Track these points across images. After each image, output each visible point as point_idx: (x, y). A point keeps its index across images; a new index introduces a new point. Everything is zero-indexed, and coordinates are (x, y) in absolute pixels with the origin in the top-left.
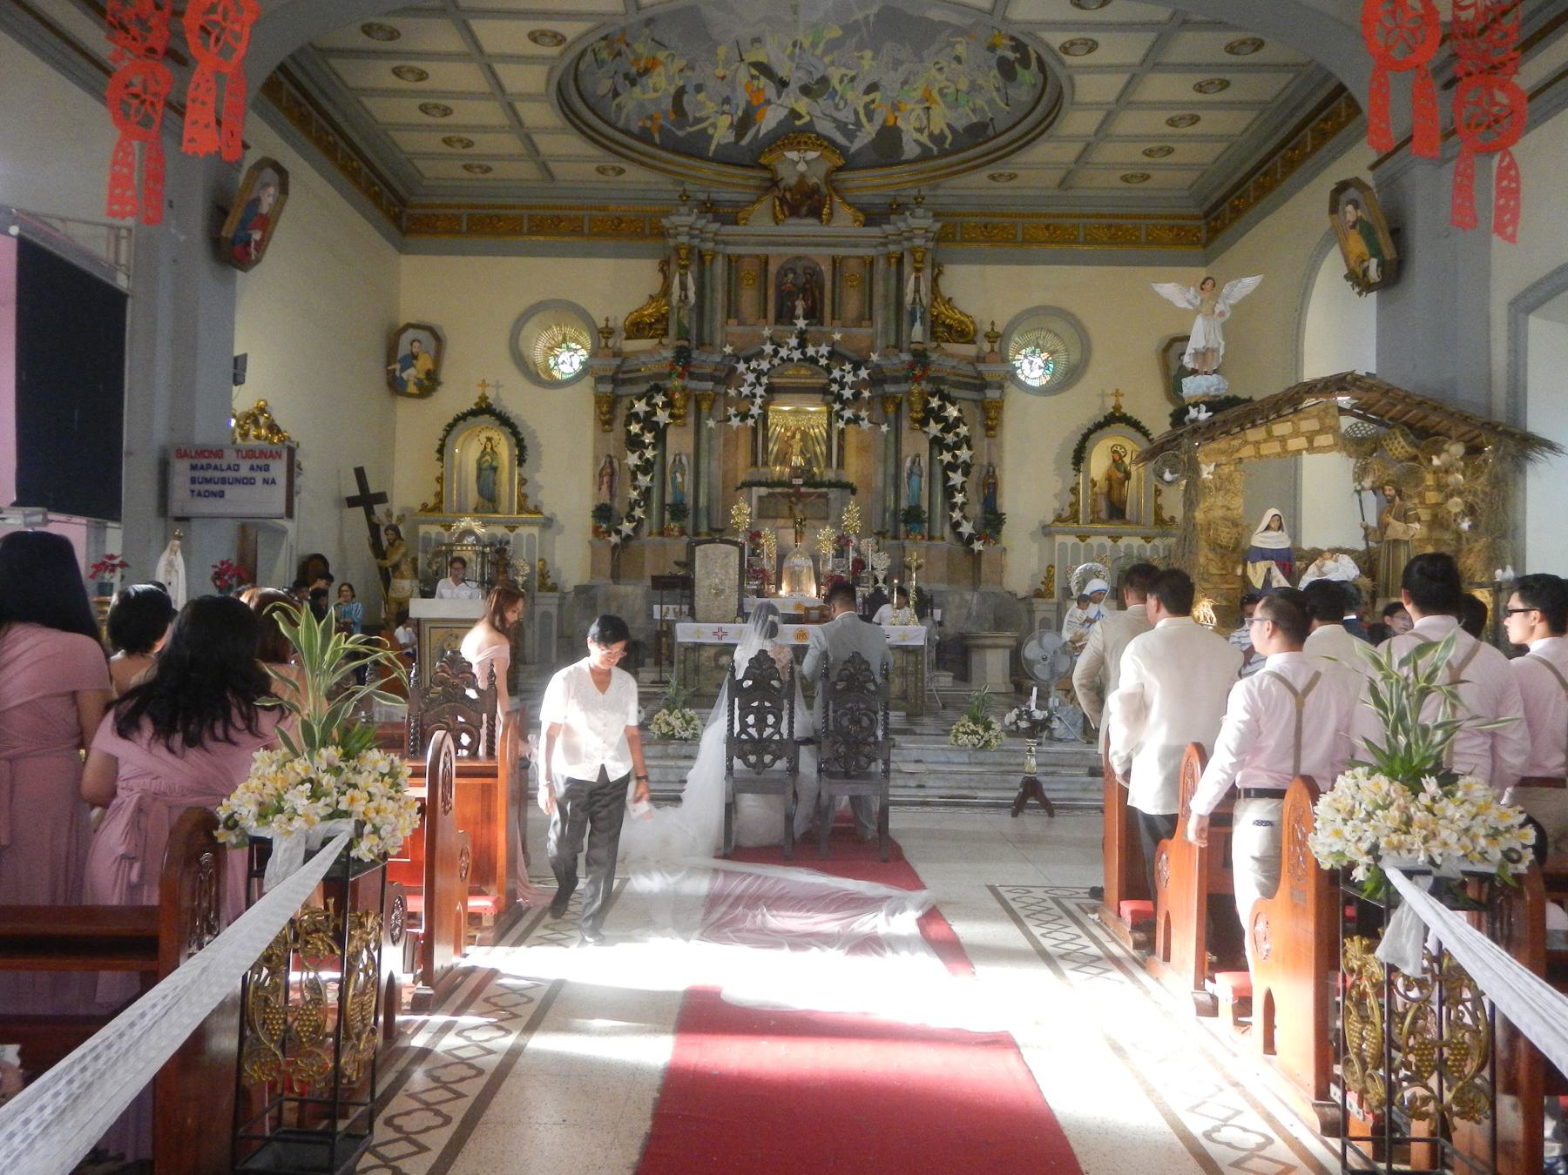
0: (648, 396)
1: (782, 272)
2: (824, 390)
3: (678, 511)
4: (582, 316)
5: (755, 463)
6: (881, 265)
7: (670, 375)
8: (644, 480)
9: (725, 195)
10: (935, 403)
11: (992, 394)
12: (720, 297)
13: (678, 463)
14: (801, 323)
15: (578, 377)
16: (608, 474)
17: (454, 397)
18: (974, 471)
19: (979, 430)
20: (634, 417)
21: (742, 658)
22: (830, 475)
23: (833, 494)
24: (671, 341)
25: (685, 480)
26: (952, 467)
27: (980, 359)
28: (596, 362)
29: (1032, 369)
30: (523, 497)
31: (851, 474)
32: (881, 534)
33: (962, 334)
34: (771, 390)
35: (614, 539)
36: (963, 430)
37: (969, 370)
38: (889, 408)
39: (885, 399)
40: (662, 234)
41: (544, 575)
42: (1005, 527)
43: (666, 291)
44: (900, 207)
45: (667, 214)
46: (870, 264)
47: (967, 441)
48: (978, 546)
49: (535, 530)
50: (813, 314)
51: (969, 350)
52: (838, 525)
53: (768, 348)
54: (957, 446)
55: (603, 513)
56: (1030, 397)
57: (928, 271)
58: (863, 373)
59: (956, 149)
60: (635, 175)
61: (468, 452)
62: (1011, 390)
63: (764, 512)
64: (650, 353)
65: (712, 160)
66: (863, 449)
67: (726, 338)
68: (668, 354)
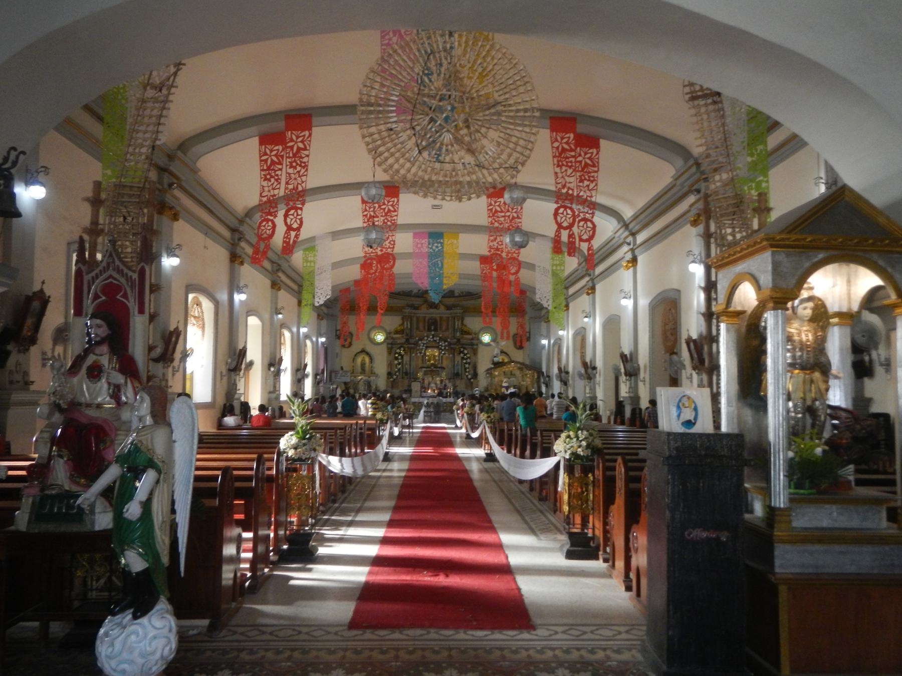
0: (400, 348)
2: (437, 347)
3: (406, 373)
4: (385, 331)
5: (423, 363)
7: (405, 343)
9: (417, 303)
10: (462, 349)
11: (475, 347)
14: (433, 333)
15: (382, 343)
16: (390, 365)
17: (357, 347)
18: (471, 364)
20: (397, 353)
22: (439, 366)
23: (440, 370)
25: (407, 367)
26: (466, 363)
27: (472, 339)
29: (486, 338)
30: (372, 370)
31: (445, 363)
32: (450, 379)
33: (468, 333)
34: (427, 347)
36: (468, 355)
38: (452, 350)
39: (452, 348)
41: (376, 388)
43: (403, 324)
46: (448, 318)
50: (436, 330)
51: (470, 337)
57: (460, 321)
59: (465, 296)
60: (396, 301)
61: (359, 360)
62: (480, 346)
63: (425, 373)
65: (414, 296)
68: (403, 340)
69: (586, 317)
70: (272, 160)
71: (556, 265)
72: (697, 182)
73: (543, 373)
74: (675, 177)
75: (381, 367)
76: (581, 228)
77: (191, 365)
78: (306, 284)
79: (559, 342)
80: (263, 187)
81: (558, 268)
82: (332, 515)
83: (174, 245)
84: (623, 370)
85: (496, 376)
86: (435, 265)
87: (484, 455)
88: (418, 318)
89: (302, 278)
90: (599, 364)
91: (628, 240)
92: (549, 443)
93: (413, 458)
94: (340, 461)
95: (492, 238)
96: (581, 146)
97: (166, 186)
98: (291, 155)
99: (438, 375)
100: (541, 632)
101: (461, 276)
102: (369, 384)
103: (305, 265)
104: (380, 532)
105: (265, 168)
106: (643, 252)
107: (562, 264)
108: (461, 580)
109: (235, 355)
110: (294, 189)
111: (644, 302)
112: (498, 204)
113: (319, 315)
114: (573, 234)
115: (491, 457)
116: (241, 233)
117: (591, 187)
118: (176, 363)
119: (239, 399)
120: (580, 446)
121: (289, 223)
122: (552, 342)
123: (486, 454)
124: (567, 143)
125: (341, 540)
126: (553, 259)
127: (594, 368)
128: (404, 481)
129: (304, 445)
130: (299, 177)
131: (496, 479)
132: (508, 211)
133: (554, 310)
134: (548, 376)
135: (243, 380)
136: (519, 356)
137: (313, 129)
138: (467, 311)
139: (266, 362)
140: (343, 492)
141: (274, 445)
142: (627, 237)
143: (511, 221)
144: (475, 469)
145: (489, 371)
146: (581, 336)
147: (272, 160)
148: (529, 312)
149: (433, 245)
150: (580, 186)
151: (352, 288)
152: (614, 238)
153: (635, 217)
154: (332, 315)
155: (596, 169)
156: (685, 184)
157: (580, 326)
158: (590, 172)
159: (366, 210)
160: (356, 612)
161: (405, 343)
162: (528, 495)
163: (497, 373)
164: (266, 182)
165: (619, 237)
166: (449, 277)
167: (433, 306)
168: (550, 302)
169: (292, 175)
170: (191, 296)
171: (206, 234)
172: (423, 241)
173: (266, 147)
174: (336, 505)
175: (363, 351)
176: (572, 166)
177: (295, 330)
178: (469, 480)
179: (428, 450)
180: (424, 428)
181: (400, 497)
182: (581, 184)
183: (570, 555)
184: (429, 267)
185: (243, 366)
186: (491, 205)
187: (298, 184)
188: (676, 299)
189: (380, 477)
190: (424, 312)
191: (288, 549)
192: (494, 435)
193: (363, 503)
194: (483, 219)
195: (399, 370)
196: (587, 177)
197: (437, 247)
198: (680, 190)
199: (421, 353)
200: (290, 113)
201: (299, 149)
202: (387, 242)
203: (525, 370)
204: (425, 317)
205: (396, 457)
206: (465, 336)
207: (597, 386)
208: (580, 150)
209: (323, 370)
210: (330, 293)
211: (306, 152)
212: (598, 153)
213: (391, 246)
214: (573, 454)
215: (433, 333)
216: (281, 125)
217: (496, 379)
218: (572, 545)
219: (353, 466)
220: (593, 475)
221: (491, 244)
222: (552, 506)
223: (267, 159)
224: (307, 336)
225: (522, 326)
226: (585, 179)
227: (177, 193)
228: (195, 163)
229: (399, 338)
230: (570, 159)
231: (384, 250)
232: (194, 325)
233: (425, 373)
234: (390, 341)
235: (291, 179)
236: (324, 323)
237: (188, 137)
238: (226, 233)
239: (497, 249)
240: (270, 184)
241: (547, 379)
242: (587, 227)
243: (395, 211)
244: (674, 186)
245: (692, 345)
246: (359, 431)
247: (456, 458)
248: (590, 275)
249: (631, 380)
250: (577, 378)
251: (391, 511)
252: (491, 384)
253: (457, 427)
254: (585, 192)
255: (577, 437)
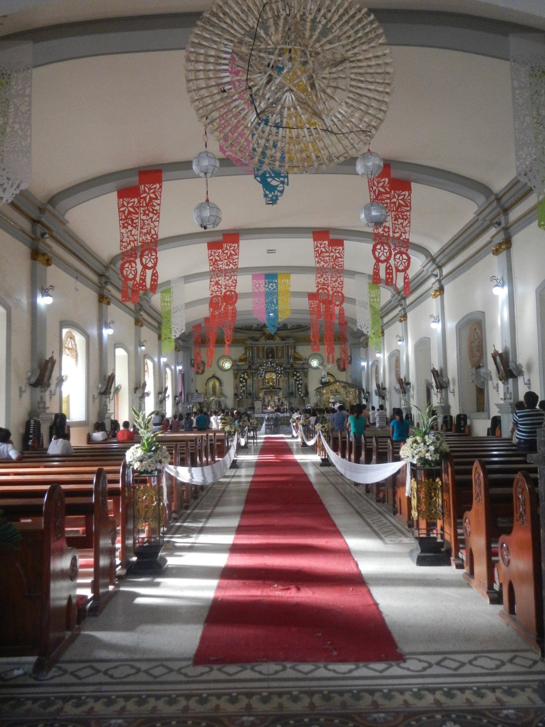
1: (267, 349)
2: (275, 372)
3: (250, 394)
6: (285, 348)
7: (248, 370)
8: (244, 389)
9: (256, 335)
10: (295, 373)
11: (306, 370)
12: (256, 354)
13: (249, 386)
16: (236, 387)
19: (304, 377)
20: (241, 377)
21: (266, 417)
22: (277, 387)
24: (247, 363)
25: (251, 388)
26: (299, 384)
27: (303, 364)
28: (234, 367)
29: (315, 363)
30: (221, 392)
31: (281, 386)
32: (286, 398)
33: (300, 359)
34: (266, 372)
35: (238, 399)
36: (300, 378)
37: (301, 366)
38: (287, 374)
39: (286, 372)
40: (245, 343)
41: (226, 406)
42: (310, 395)
43: (246, 353)
44: (288, 337)
45: (246, 341)
47: (301, 379)
48: (304, 398)
49: (224, 398)
50: (273, 357)
51: (301, 362)
52: (278, 396)
53: (265, 364)
54: (299, 380)
55: (236, 395)
56: (313, 370)
58: (282, 368)
61: (211, 384)
62: (310, 370)
63: (265, 394)
64: (244, 365)
66: (283, 381)
67: (257, 360)
68: (247, 366)
69: (400, 340)
70: (129, 211)
71: (373, 298)
72: (498, 215)
73: (363, 390)
74: (477, 213)
75: (229, 389)
76: (398, 260)
77: (66, 389)
78: (164, 322)
79: (376, 365)
80: (122, 233)
81: (375, 300)
82: (184, 522)
83: (48, 286)
84: (434, 384)
85: (324, 394)
86: (272, 302)
87: (321, 461)
88: (258, 348)
89: (161, 316)
90: (412, 379)
91: (435, 273)
92: (386, 448)
93: (258, 465)
94: (190, 471)
95: (319, 275)
96: (395, 189)
97: (39, 235)
98: (144, 205)
99: (276, 394)
100: (413, 665)
101: (294, 312)
102: (219, 404)
103: (163, 304)
104: (229, 539)
105: (123, 217)
106: (448, 283)
107: (378, 296)
108: (313, 593)
109: (105, 380)
110: (147, 233)
111: (451, 325)
112: (323, 246)
113: (176, 348)
114: (390, 266)
115: (326, 462)
116: (107, 278)
117: (404, 225)
118: (52, 387)
119: (109, 418)
120: (428, 451)
121: (144, 263)
122: (370, 363)
123: (322, 459)
124: (383, 187)
125: (191, 549)
126: (370, 292)
127: (408, 384)
128: (250, 486)
129: (150, 457)
130: (152, 222)
131: (333, 482)
132: (332, 252)
133: (372, 336)
134: (368, 393)
135: (112, 402)
136: (342, 376)
137: (163, 183)
138: (298, 341)
139: (133, 386)
140: (196, 498)
141: (120, 457)
142: (434, 270)
143: (334, 260)
144: (311, 472)
145: (318, 390)
146: (395, 358)
147: (129, 211)
148: (350, 340)
149: (269, 285)
150: (394, 224)
151: (203, 325)
152: (423, 271)
153: (442, 251)
154: (188, 348)
155: (408, 209)
156: (487, 219)
157: (394, 348)
158: (403, 212)
159: (211, 255)
160: (204, 639)
161: (248, 370)
162: (365, 497)
163: (325, 392)
164: (125, 229)
165: (427, 270)
166: (283, 312)
167: (270, 337)
168: (369, 329)
169: (146, 222)
170: (65, 331)
171: (77, 278)
172: (261, 282)
173: (123, 200)
174: (189, 511)
175: (214, 377)
176: (387, 207)
177: (156, 360)
178: (310, 483)
179: (270, 457)
180: (266, 438)
181: (248, 502)
182: (396, 222)
183: (421, 561)
184: (266, 303)
185: (112, 390)
186: (317, 247)
187: (151, 228)
188: (481, 321)
189: (229, 483)
190: (263, 343)
191: (137, 562)
192: (328, 442)
193: (213, 509)
194: (311, 261)
195: (244, 391)
196: (400, 216)
197: (272, 286)
198: (481, 225)
199: (261, 377)
200: (143, 170)
201: (151, 199)
202: (230, 281)
203: (348, 388)
204: (264, 347)
205: (243, 464)
206: (297, 362)
207: (411, 399)
208: (394, 192)
209: (181, 393)
210: (184, 328)
211: (158, 202)
212: (409, 194)
213: (233, 285)
214: (420, 459)
215: (271, 360)
216: (135, 180)
217: (324, 396)
218: (422, 551)
219: (203, 475)
220: (441, 480)
221: (319, 280)
222: (391, 507)
223: (125, 210)
224: (167, 365)
225: (344, 351)
226: (399, 218)
227: (49, 241)
228: (64, 216)
229: (243, 365)
230: (386, 201)
231: (228, 288)
232: (68, 355)
233: (265, 394)
234: (236, 368)
235: (144, 224)
236: (181, 353)
237: (55, 192)
238: (95, 278)
239: (324, 284)
240: (127, 230)
241: (367, 394)
242: (403, 259)
243: (236, 254)
244: (478, 220)
245: (498, 358)
246: (209, 443)
247: (295, 464)
248: (402, 305)
249: (442, 392)
250: (394, 392)
251: (235, 533)
252: (320, 400)
253: (293, 437)
254: (399, 228)
255: (425, 442)
